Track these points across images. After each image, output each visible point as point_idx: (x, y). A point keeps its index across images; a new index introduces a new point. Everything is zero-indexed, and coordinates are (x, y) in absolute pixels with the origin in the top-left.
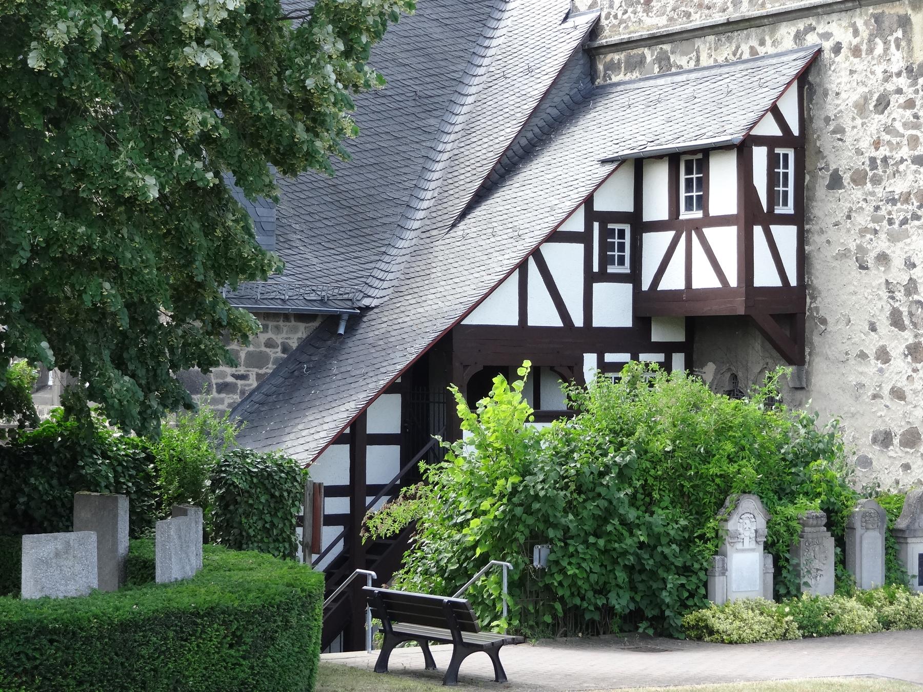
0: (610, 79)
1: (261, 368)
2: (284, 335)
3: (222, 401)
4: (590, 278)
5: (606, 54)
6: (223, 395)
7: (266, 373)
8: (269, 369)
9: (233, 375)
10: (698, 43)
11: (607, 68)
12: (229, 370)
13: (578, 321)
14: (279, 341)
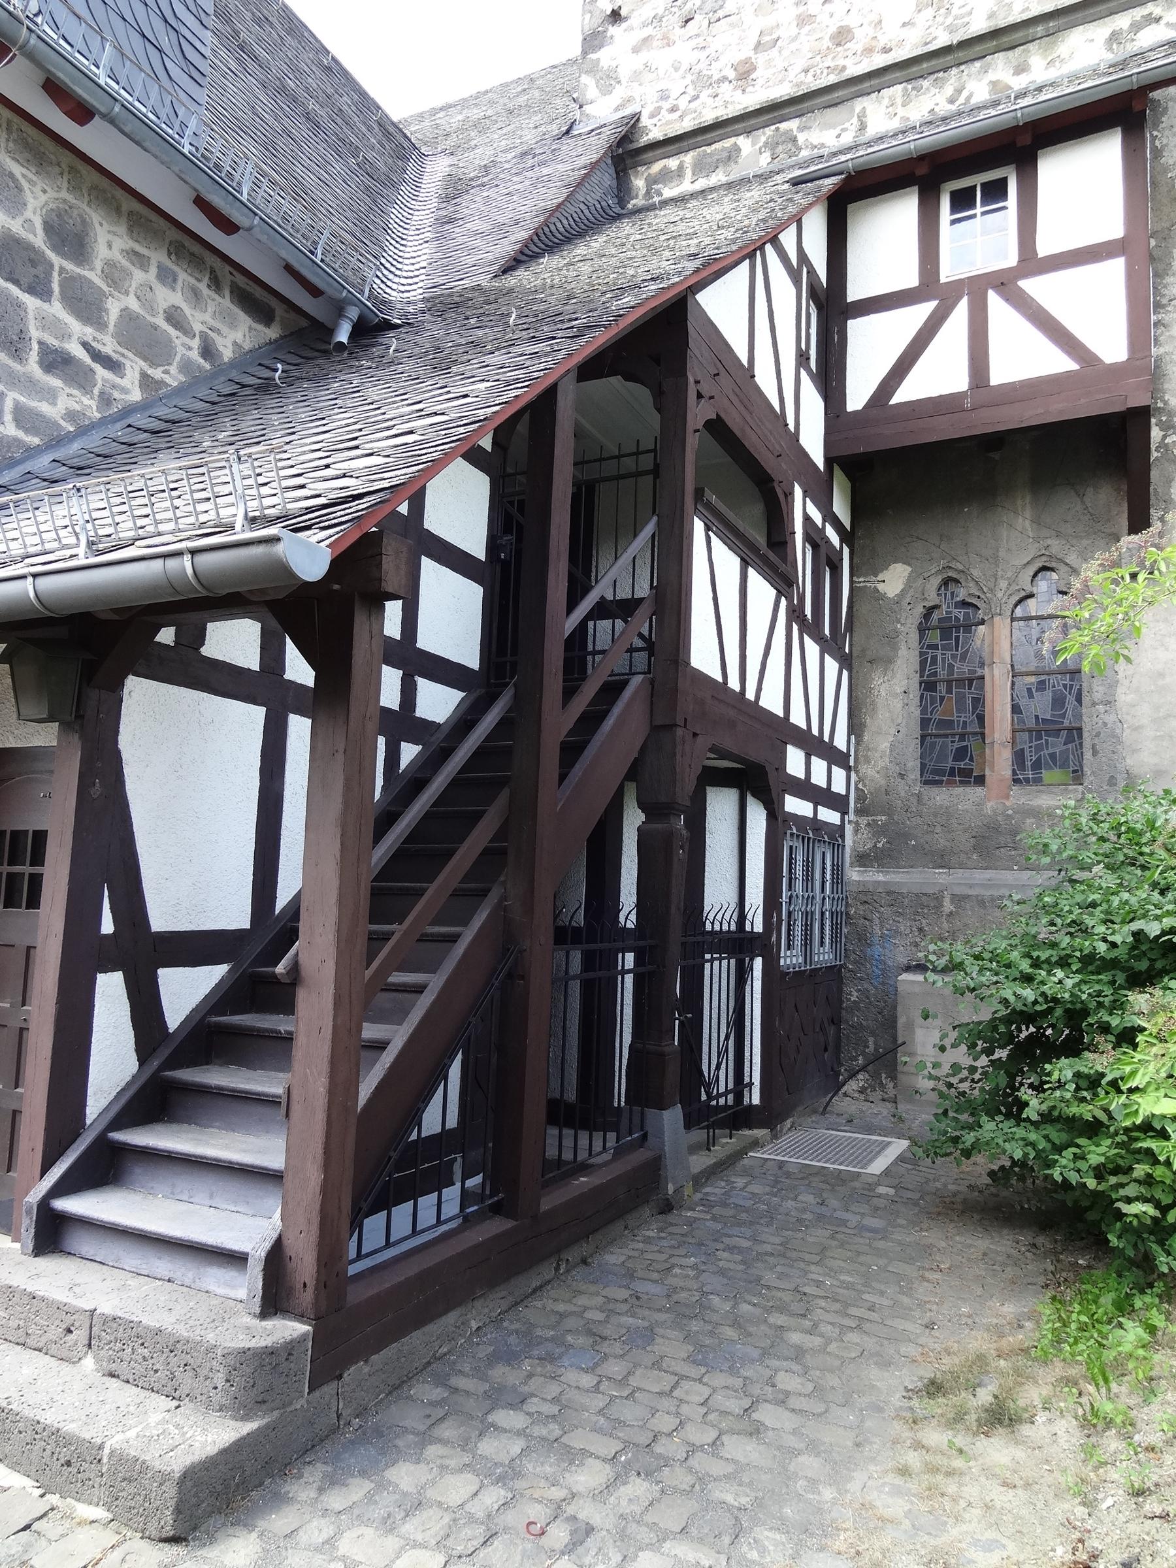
0: (659, 194)
1: (153, 365)
2: (207, 317)
3: (51, 396)
5: (650, 163)
6: (55, 382)
7: (162, 383)
8: (172, 377)
9: (85, 345)
10: (859, 104)
11: (652, 181)
12: (76, 327)
14: (197, 327)
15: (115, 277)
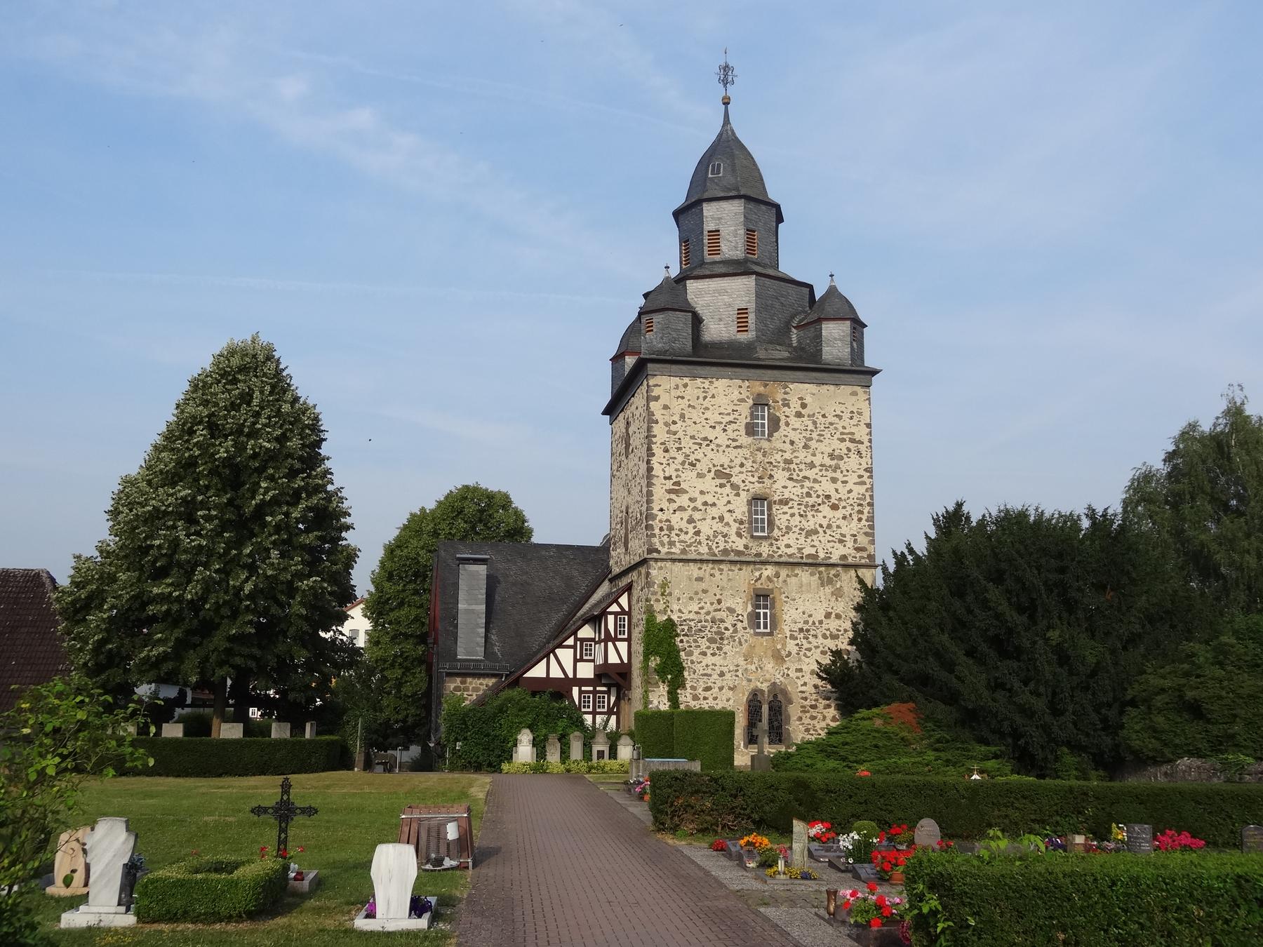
4: (576, 661)
8: (481, 693)
13: (571, 676)
15: (471, 683)
